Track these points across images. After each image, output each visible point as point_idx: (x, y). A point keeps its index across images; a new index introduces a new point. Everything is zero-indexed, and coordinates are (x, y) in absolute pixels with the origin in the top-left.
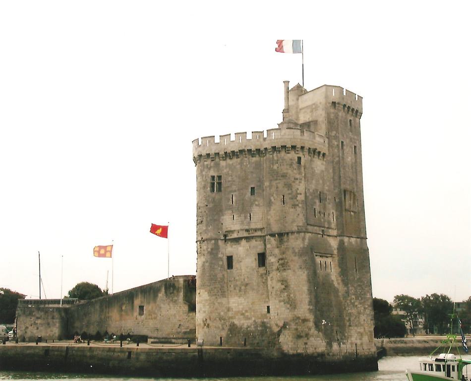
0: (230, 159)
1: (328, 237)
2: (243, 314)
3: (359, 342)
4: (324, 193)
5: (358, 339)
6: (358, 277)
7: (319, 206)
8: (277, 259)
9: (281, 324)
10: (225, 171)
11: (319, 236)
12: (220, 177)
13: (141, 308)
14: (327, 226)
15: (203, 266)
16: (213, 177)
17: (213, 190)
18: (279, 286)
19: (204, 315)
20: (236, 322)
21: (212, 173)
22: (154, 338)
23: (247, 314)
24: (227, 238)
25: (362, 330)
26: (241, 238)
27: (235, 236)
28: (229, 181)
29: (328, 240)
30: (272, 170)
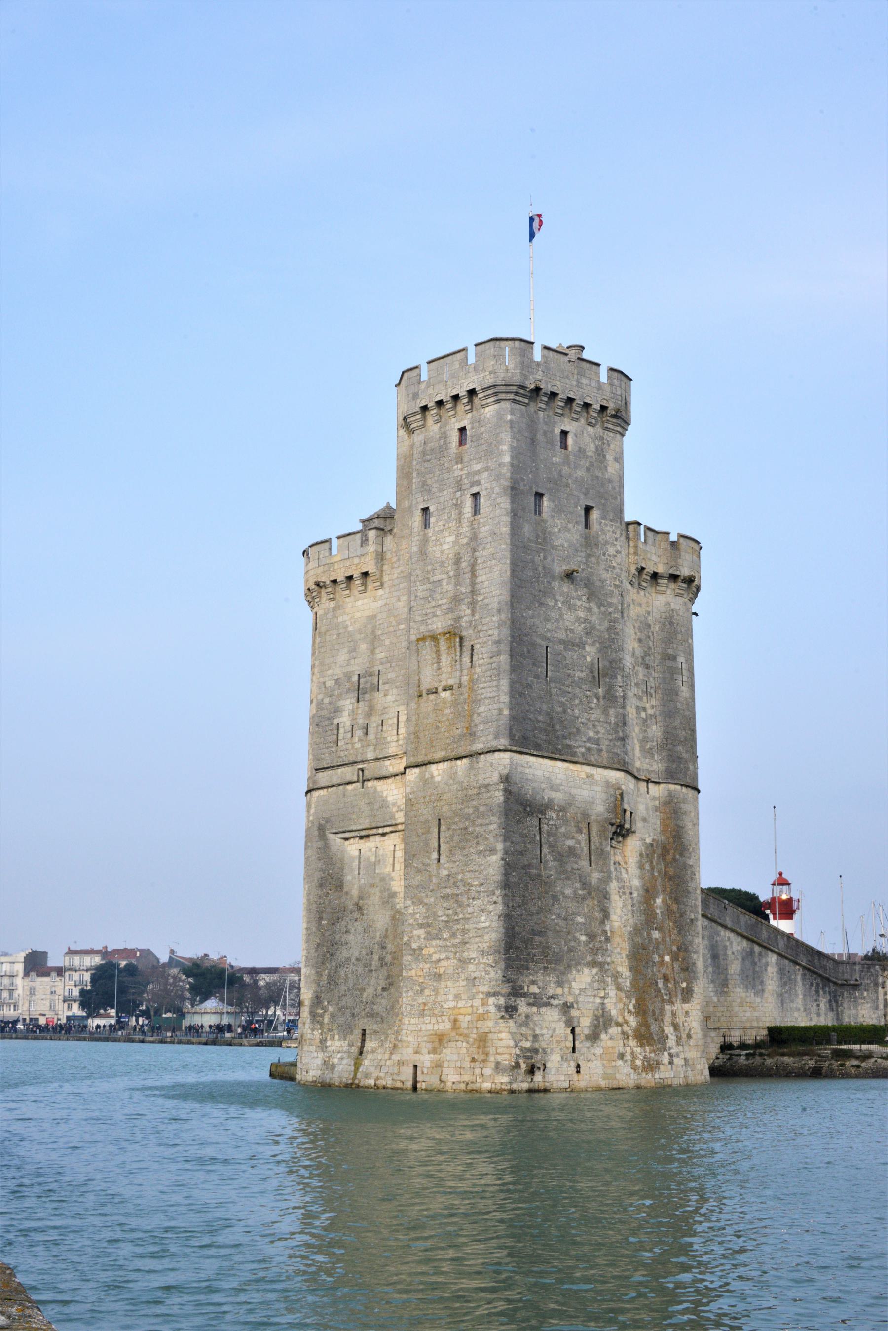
1: (379, 785)
3: (426, 1060)
4: (371, 675)
5: (425, 1051)
6: (445, 872)
7: (353, 713)
11: (350, 787)
14: (370, 755)
25: (445, 1026)
29: (379, 789)
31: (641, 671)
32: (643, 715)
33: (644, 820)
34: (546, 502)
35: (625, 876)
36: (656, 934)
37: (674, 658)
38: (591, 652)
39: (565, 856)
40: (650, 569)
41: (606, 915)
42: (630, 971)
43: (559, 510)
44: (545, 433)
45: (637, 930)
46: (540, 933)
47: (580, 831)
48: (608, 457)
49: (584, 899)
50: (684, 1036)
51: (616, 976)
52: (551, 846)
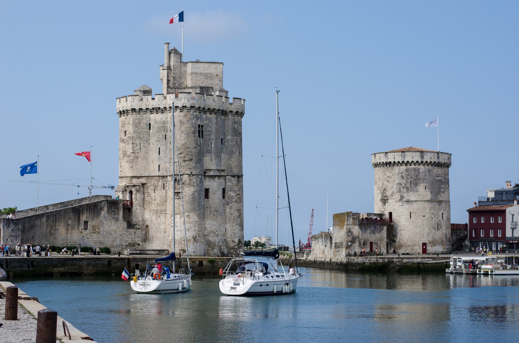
0: (210, 114)
2: (214, 233)
8: (236, 194)
9: (237, 240)
10: (205, 122)
12: (202, 126)
13: (86, 223)
15: (193, 194)
16: (199, 125)
17: (199, 136)
18: (236, 214)
19: (195, 232)
20: (210, 238)
21: (199, 122)
22: (139, 250)
23: (217, 233)
24: (206, 175)
26: (216, 176)
27: (212, 173)
28: (209, 131)
30: (234, 128)
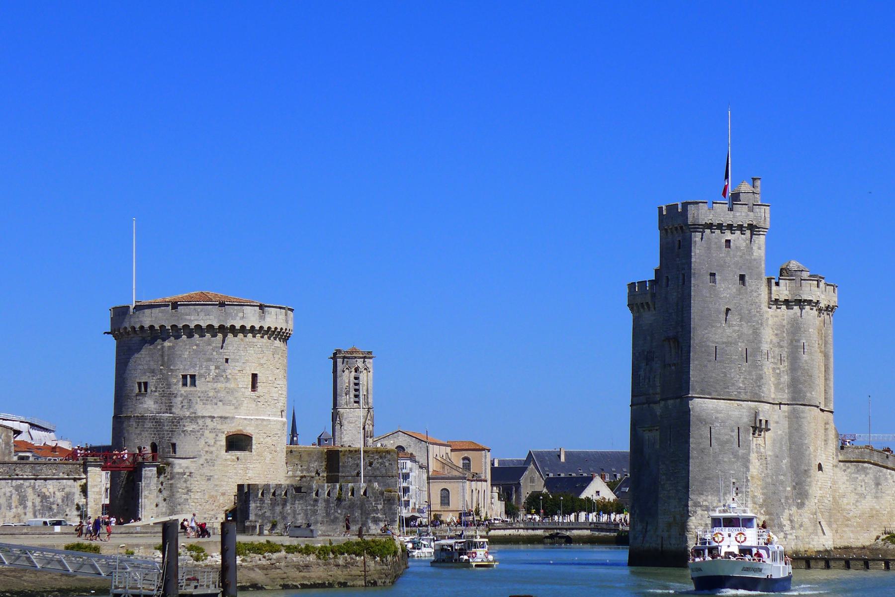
25: (671, 520)
31: (777, 350)
32: (778, 371)
33: (777, 423)
34: (717, 277)
35: (762, 450)
36: (782, 477)
37: (798, 341)
38: (741, 346)
39: (723, 444)
40: (782, 298)
41: (748, 469)
42: (763, 494)
43: (724, 280)
44: (716, 243)
45: (767, 476)
46: (709, 479)
47: (733, 431)
48: (755, 248)
49: (734, 463)
50: (797, 526)
51: (754, 497)
52: (716, 439)
